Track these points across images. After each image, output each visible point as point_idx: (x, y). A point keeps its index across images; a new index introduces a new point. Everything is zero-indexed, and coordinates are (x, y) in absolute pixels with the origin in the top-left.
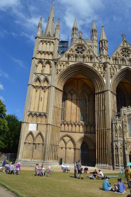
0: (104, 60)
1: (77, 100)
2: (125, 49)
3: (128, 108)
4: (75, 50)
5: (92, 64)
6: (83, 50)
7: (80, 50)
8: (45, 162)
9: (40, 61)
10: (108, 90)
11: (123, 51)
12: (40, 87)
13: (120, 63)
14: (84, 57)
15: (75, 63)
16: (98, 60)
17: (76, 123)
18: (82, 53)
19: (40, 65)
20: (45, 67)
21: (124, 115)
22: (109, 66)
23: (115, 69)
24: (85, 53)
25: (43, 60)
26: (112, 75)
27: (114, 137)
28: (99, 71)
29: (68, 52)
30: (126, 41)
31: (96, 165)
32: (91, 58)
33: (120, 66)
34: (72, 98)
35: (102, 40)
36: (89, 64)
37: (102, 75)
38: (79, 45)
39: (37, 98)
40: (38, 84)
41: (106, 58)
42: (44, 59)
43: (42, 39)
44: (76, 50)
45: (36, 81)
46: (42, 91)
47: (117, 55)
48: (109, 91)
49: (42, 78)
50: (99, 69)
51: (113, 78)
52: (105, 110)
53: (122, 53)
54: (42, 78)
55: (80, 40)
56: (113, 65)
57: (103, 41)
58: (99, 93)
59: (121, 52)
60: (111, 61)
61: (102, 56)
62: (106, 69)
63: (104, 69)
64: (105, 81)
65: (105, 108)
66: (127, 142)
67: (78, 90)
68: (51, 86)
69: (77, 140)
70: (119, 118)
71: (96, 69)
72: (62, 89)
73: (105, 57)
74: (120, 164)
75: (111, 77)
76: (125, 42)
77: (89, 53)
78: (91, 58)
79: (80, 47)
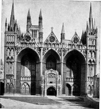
6: (30, 39)
7: (28, 39)
9: (8, 48)
11: (51, 39)
19: (9, 50)
22: (42, 49)
25: (10, 47)
39: (9, 68)
40: (9, 60)
46: (11, 64)
49: (10, 57)
57: (40, 33)
64: (39, 56)
68: (14, 61)
72: (20, 61)
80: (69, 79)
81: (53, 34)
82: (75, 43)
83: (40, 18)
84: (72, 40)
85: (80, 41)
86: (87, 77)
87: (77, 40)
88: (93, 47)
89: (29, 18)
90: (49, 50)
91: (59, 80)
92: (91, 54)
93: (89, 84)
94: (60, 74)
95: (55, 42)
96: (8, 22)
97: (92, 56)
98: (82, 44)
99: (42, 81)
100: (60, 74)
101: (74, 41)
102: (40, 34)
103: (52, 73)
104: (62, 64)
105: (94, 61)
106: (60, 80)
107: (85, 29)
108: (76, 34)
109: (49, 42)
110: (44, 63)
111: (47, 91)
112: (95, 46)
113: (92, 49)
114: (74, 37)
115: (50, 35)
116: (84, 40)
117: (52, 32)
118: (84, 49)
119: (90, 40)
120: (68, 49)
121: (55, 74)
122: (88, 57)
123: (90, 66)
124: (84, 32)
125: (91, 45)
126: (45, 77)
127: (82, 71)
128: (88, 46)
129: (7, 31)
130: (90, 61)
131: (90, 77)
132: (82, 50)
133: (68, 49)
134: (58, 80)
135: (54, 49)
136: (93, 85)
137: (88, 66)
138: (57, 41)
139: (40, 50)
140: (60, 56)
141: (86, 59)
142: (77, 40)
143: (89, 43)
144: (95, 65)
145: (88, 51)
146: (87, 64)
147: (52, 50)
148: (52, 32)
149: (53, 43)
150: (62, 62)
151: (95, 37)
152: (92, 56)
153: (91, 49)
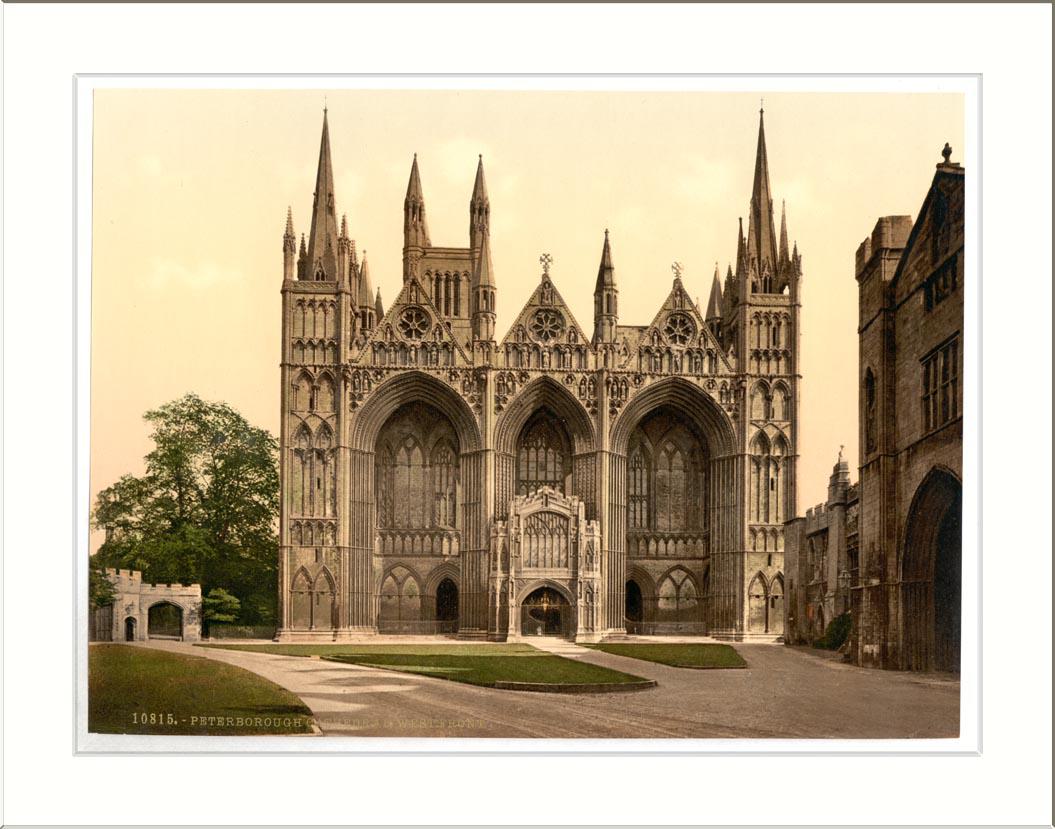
2: (547, 311)
3: (528, 497)
4: (400, 325)
8: (341, 629)
9: (306, 375)
10: (487, 451)
12: (312, 451)
15: (402, 372)
18: (419, 335)
19: (305, 386)
20: (319, 389)
22: (492, 375)
23: (510, 384)
29: (379, 338)
42: (315, 367)
43: (300, 297)
44: (404, 325)
45: (298, 435)
47: (521, 333)
49: (314, 425)
53: (536, 327)
54: (314, 425)
55: (414, 288)
57: (481, 290)
58: (467, 456)
61: (476, 344)
70: (504, 525)
81: (554, 292)
83: (479, 209)
84: (657, 325)
85: (700, 327)
86: (747, 533)
87: (683, 323)
88: (778, 359)
89: (413, 208)
90: (530, 381)
91: (591, 545)
92: (768, 399)
93: (758, 569)
94: (592, 514)
95: (564, 340)
96: (303, 229)
97: (769, 413)
98: (711, 345)
99: (495, 554)
100: (592, 514)
101: (669, 330)
102: (478, 294)
103: (549, 512)
104: (606, 460)
106: (597, 546)
107: (729, 260)
108: (679, 291)
113: (773, 372)
114: (670, 306)
115: (537, 302)
116: (726, 330)
117: (546, 283)
118: (727, 372)
119: (760, 323)
120: (639, 377)
121: (567, 513)
122: (748, 418)
123: (763, 470)
124: (723, 279)
125: (766, 353)
126: (513, 531)
129: (296, 278)
131: (763, 530)
132: (710, 377)
133: (639, 377)
134: (582, 551)
135: (558, 377)
136: (779, 577)
137: (749, 468)
138: (575, 330)
139: (482, 384)
142: (683, 323)
143: (754, 337)
144: (791, 460)
145: (750, 385)
146: (743, 456)
147: (546, 384)
148: (546, 283)
149: (552, 342)
150: (607, 447)
151: (787, 302)
152: (769, 413)
153: (763, 371)
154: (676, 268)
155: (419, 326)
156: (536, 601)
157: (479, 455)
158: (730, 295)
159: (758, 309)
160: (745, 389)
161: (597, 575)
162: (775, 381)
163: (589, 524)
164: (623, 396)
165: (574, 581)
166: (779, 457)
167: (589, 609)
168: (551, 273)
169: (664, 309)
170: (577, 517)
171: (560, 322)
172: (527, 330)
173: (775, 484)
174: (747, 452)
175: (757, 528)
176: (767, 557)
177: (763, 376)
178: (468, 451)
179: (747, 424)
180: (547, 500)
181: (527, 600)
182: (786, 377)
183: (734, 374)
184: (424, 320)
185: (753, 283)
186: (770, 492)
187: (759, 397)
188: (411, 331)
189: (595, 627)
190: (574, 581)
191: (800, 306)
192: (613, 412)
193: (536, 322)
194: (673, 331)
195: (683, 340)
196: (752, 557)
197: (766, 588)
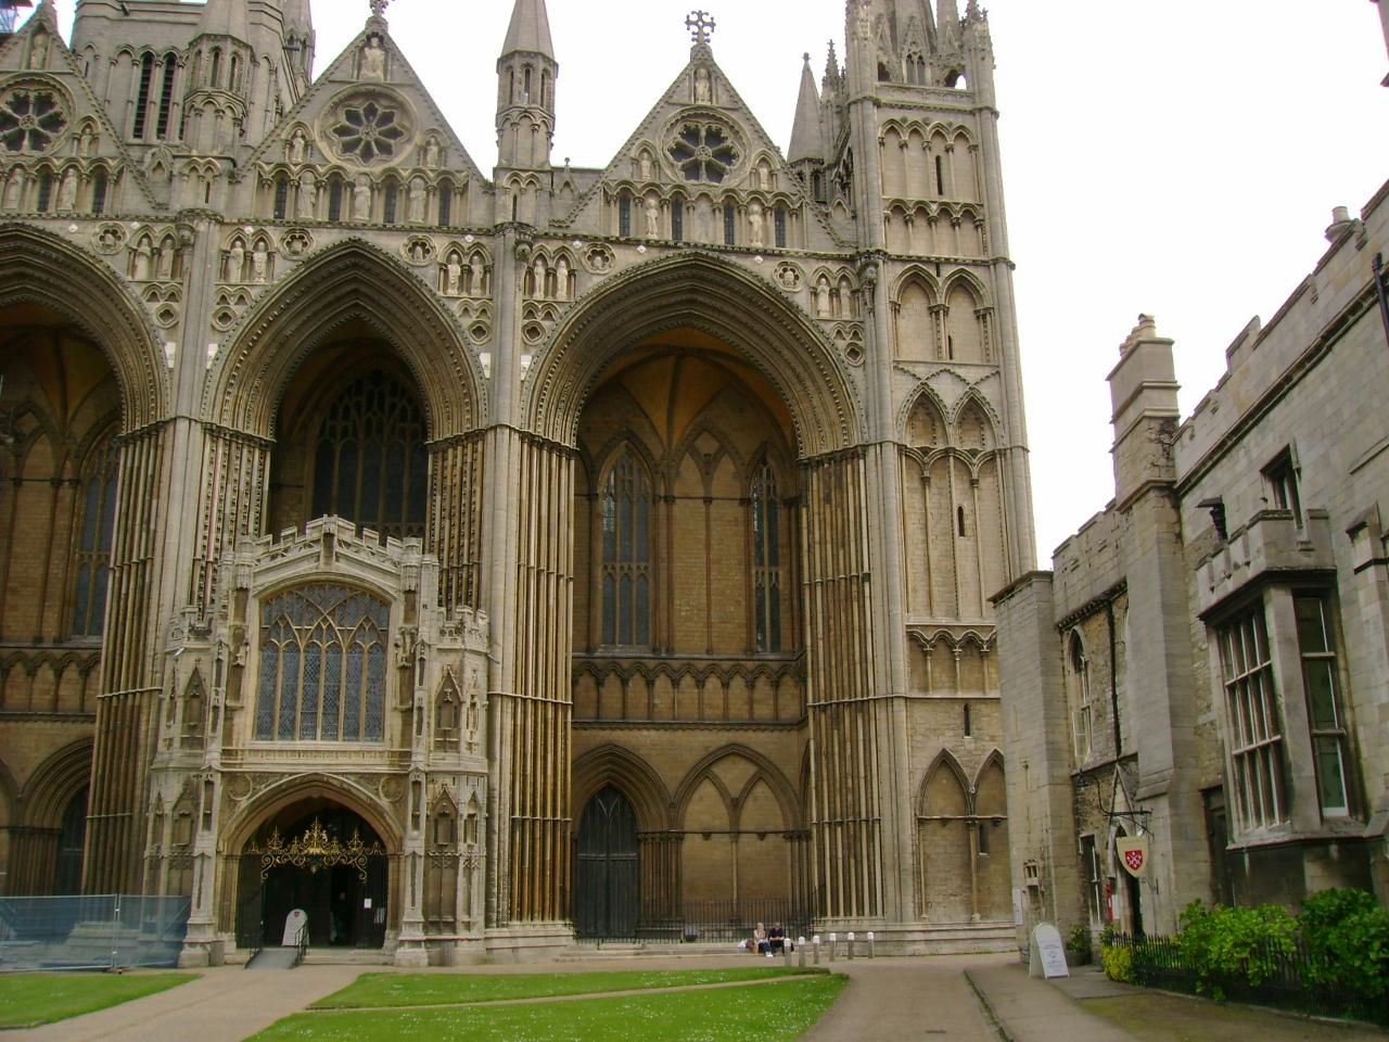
0: (187, 195)
1: (57, 483)
3: (276, 540)
5: (97, 228)
6: (55, 122)
11: (352, 116)
13: (309, 205)
14: (47, 178)
16: (146, 191)
17: (32, 653)
18: (38, 140)
21: (243, 591)
23: (260, 257)
24: (60, 149)
26: (232, 301)
27: (161, 746)
28: (135, 276)
30: (381, 39)
31: (77, 930)
32: (100, 178)
33: (298, 233)
34: (20, 467)
35: (225, 37)
36: (74, 227)
37: (154, 308)
38: (28, 80)
41: (209, 176)
47: (299, 143)
48: (182, 425)
50: (142, 264)
51: (229, 325)
52: (144, 563)
53: (342, 131)
55: (40, 39)
56: (249, 230)
59: (332, 121)
60: (248, 200)
61: (178, 165)
62: (186, 258)
63: (178, 255)
64: (170, 349)
65: (146, 555)
66: (217, 779)
67: (65, 407)
69: (28, 773)
71: (117, 264)
73: (201, 172)
74: (158, 920)
75: (225, 317)
76: (375, 41)
77: (95, 139)
78: (100, 178)
79: (32, 95)
80: (637, 685)
82: (692, 170)
92: (934, 311)
98: (784, 185)
101: (679, 151)
105: (974, 411)
108: (702, 64)
109: (330, 154)
110: (237, 439)
111: (248, 863)
112: (969, 212)
119: (903, 146)
120: (600, 248)
122: (888, 356)
125: (922, 209)
127: (817, 562)
128: (879, 211)
130: (925, 406)
133: (600, 248)
134: (427, 692)
135: (394, 245)
138: (441, 134)
140: (479, 331)
141: (857, 374)
143: (893, 173)
145: (889, 277)
149: (377, 168)
150: (513, 409)
153: (919, 250)
154: (700, 24)
155: (43, 124)
156: (287, 841)
157: (156, 431)
158: (835, 102)
159: (897, 115)
160: (872, 285)
161: (475, 761)
162: (947, 271)
163: (449, 618)
164: (562, 295)
165: (400, 781)
166: (974, 453)
167: (441, 859)
168: (387, 14)
169: (667, 100)
170: (410, 594)
171: (406, 123)
172: (315, 135)
173: (967, 522)
174: (892, 435)
175: (929, 635)
176: (959, 709)
177: (919, 259)
178: (138, 427)
179: (887, 372)
180: (329, 547)
181: (261, 836)
182: (975, 263)
183: (848, 252)
184: (57, 109)
185: (881, 66)
186: (959, 541)
187: (916, 305)
188: (21, 135)
189: (462, 917)
190: (400, 781)
191: (996, 114)
192: (533, 331)
193: (344, 121)
194: (690, 154)
195: (716, 174)
196: (920, 712)
197: (968, 800)
